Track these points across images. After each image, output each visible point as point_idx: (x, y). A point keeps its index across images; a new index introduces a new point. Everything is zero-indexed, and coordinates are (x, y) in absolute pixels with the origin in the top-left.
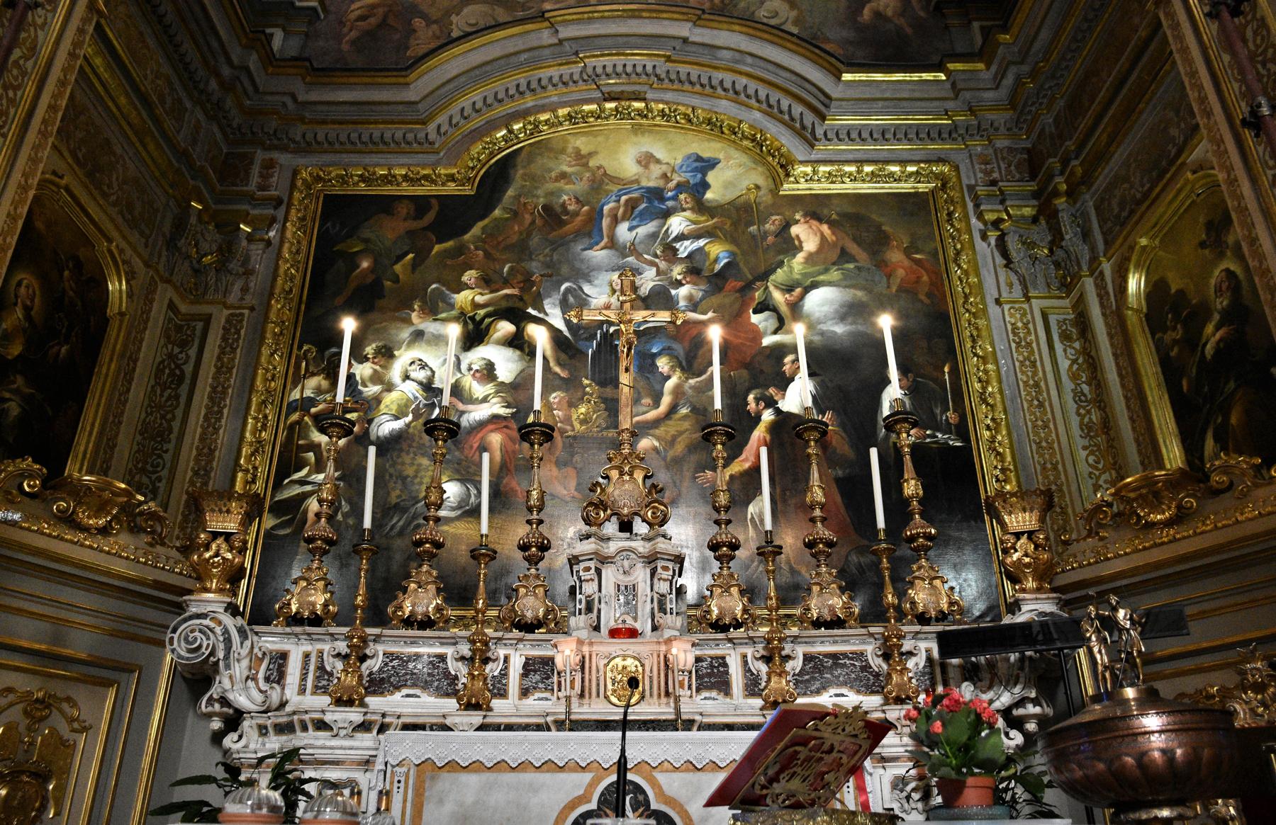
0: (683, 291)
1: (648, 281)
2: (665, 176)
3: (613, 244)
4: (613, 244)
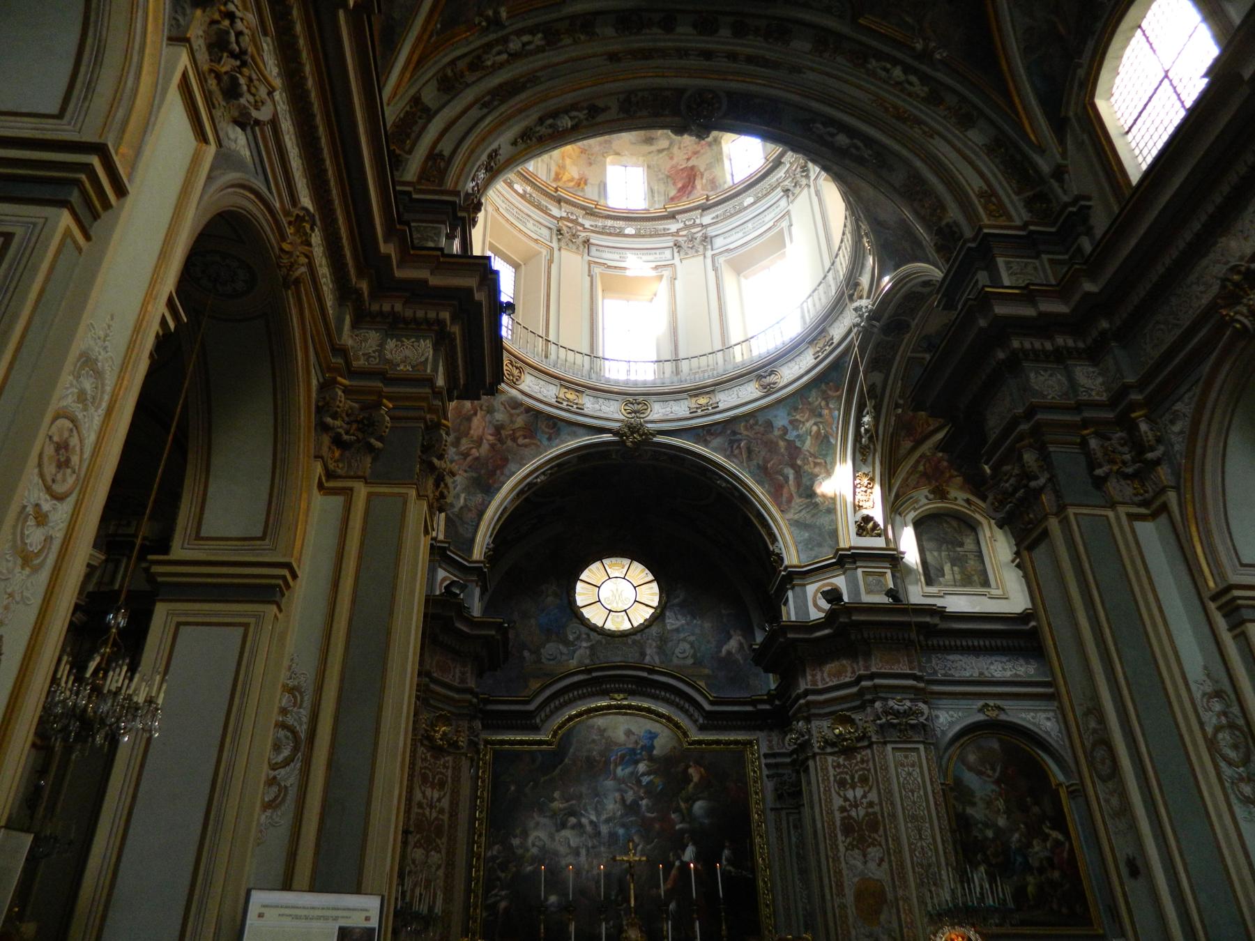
0: (644, 802)
1: (630, 796)
2: (636, 743)
3: (615, 778)
4: (615, 778)
